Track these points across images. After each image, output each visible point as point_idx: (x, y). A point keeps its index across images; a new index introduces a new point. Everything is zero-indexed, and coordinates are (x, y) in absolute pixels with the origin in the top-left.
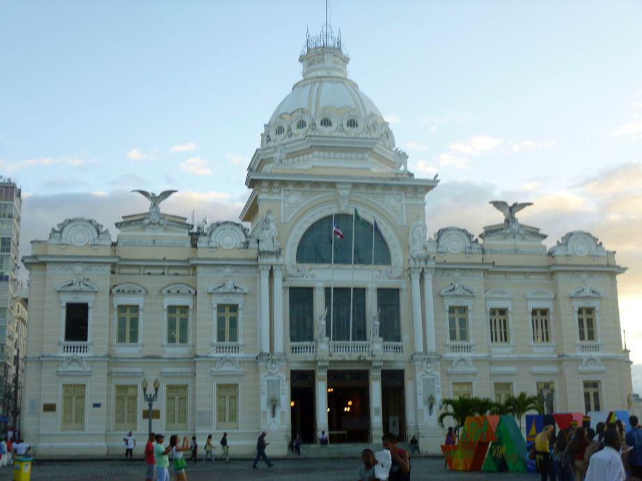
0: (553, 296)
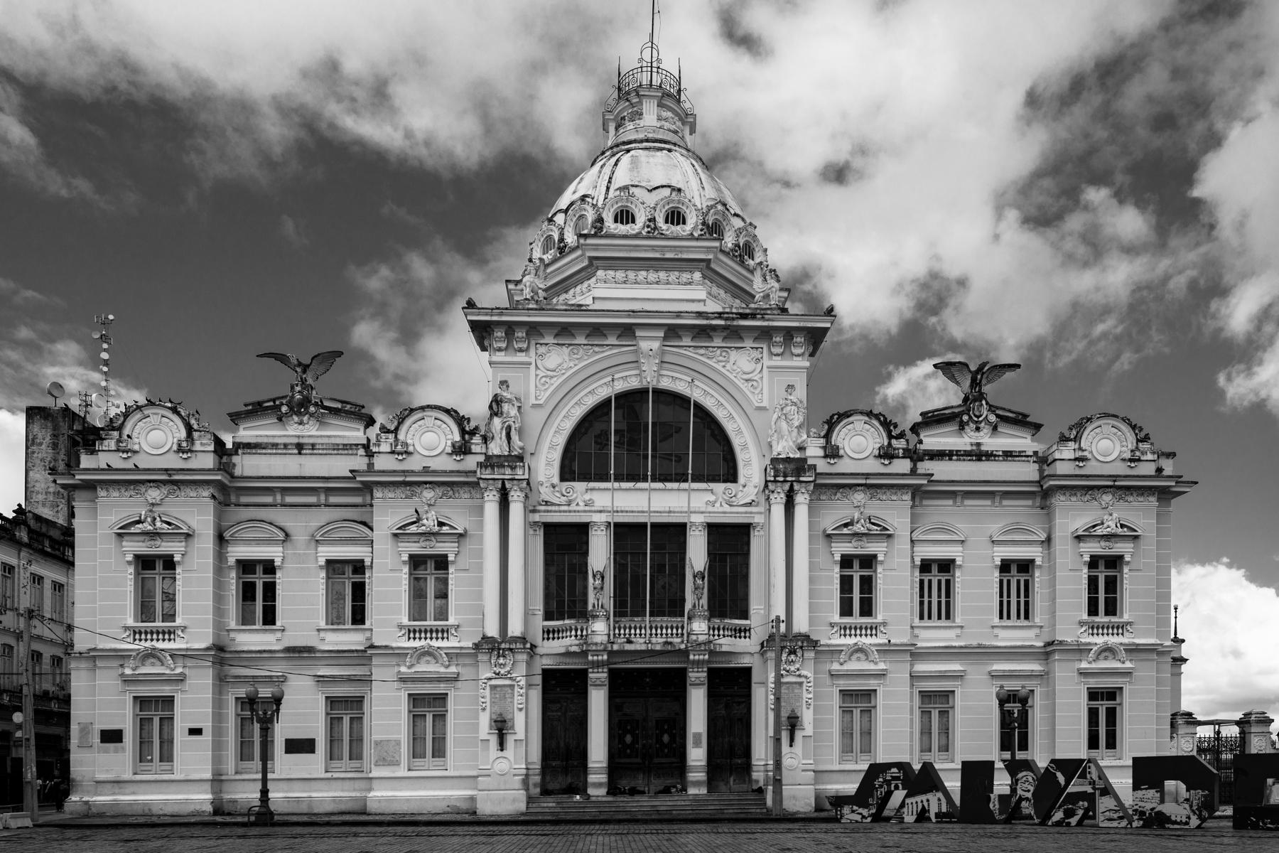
0: (1043, 537)
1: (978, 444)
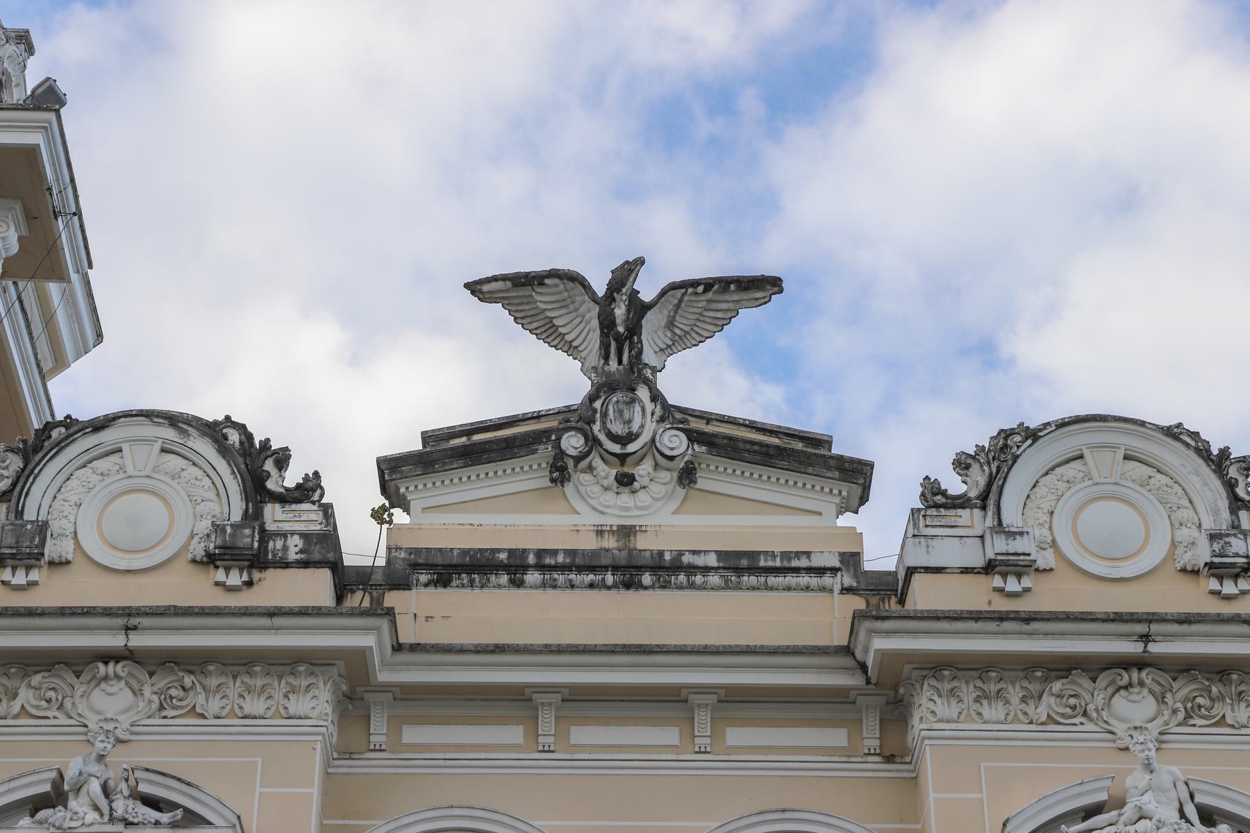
1: (627, 532)
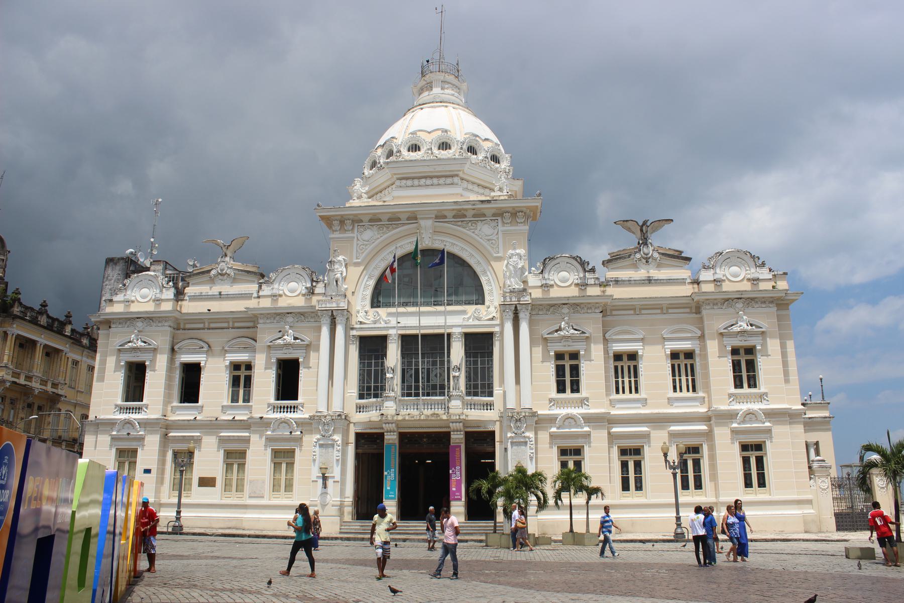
0: (699, 333)
